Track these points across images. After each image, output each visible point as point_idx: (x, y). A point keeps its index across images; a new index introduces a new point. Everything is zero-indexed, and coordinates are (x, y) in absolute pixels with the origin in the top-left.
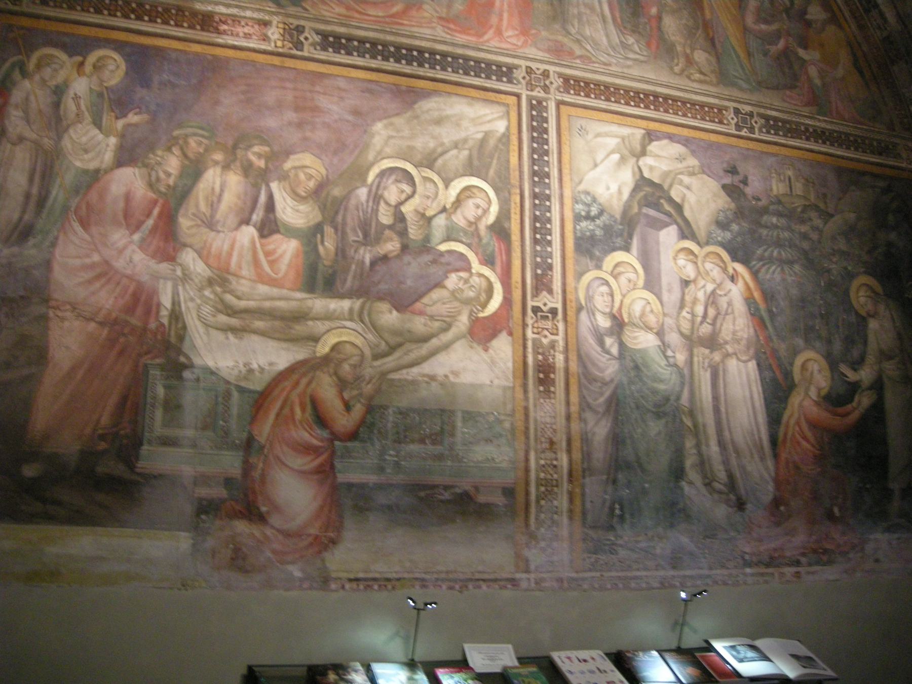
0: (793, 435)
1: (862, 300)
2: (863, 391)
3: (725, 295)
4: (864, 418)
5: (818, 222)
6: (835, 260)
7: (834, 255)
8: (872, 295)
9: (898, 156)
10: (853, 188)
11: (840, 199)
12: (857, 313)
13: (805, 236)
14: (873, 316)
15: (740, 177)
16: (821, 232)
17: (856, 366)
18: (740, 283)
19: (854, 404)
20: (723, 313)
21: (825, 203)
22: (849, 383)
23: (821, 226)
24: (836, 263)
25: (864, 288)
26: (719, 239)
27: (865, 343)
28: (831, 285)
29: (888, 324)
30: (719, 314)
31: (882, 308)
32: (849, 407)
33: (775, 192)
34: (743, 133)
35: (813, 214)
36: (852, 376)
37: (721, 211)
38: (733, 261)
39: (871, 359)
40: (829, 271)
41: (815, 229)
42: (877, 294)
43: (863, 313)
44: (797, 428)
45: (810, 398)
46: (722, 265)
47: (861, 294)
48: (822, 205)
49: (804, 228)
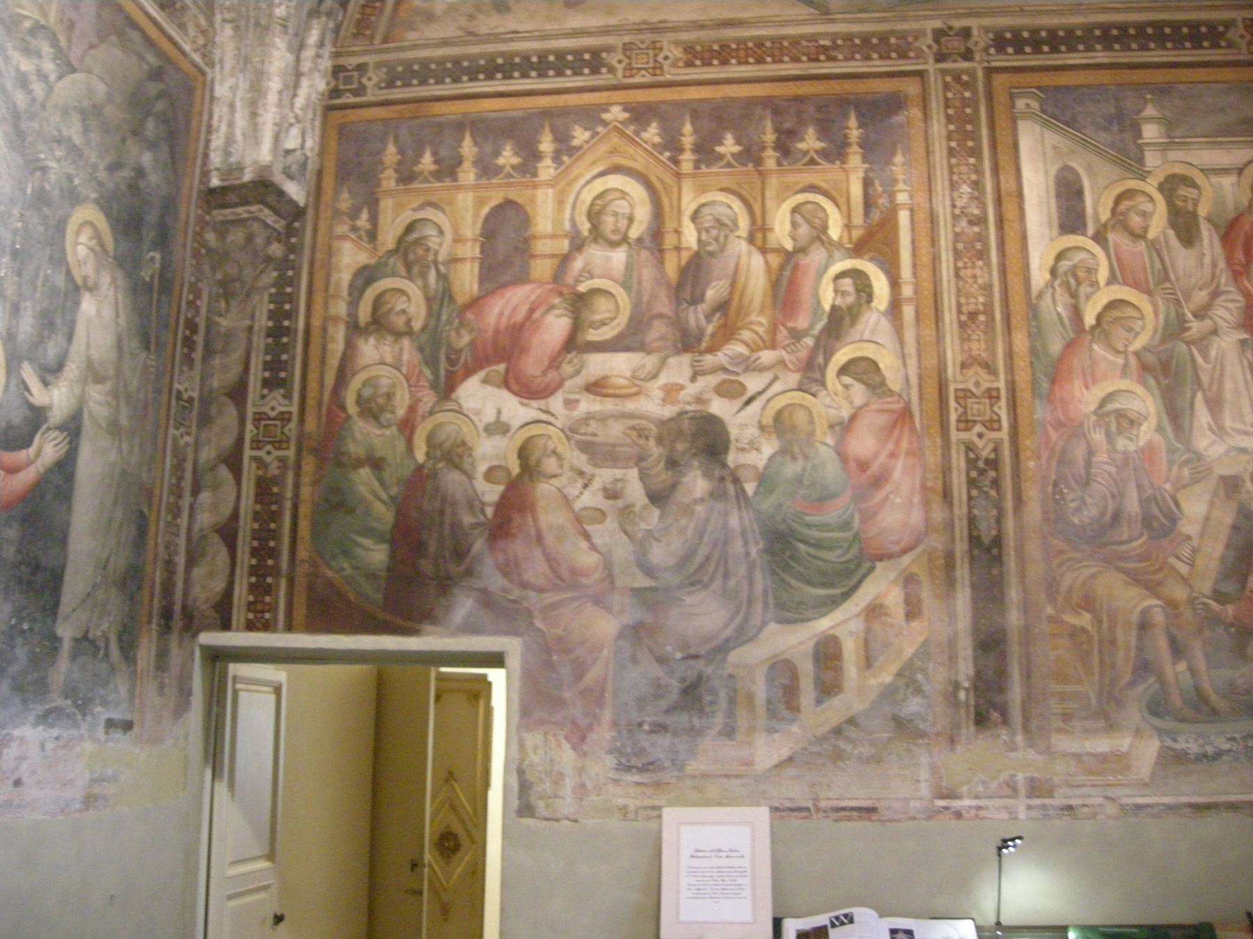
1: (82, 251)
2: (49, 429)
4: (38, 488)
5: (49, 67)
6: (59, 153)
7: (59, 142)
8: (97, 248)
9: (182, 27)
10: (113, 38)
11: (92, 46)
12: (68, 273)
13: (23, 81)
14: (90, 290)
16: (50, 88)
17: (49, 377)
21: (69, 41)
22: (32, 407)
23: (52, 77)
24: (58, 161)
27: (70, 337)
28: (41, 198)
29: (108, 313)
31: (106, 279)
35: (46, 49)
36: (39, 395)
39: (72, 369)
40: (44, 169)
41: (43, 77)
42: (104, 250)
43: (79, 281)
47: (83, 238)
48: (63, 41)
49: (26, 65)
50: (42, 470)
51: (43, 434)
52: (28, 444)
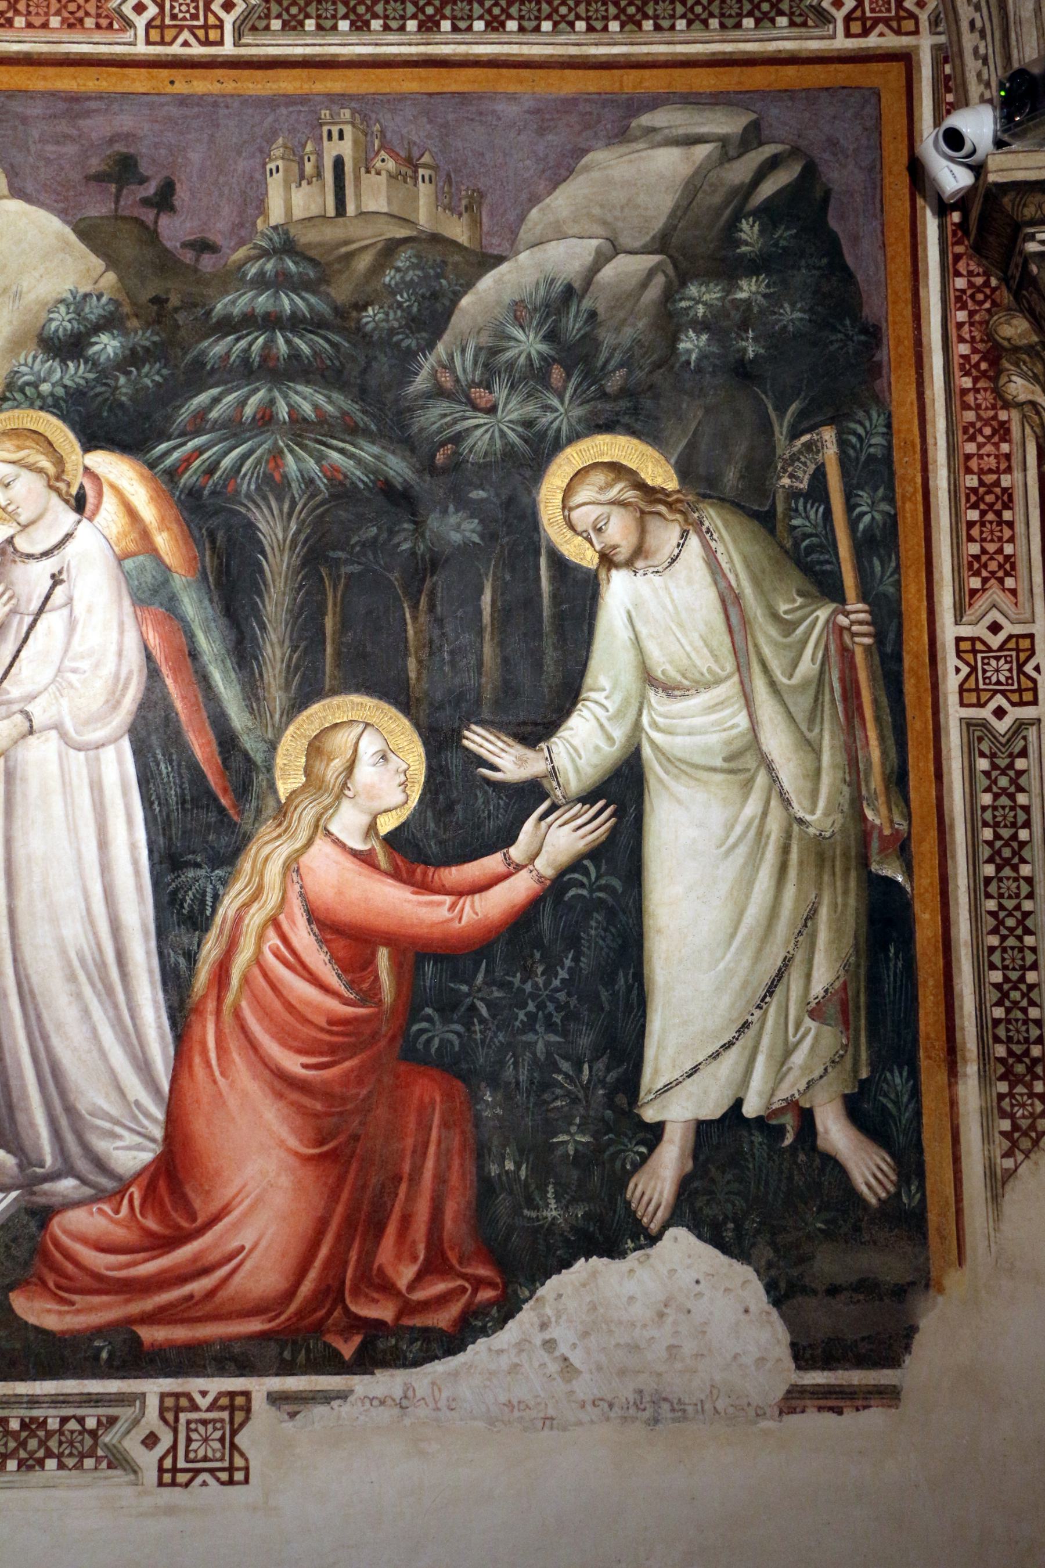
0: (258, 960)
2: (554, 808)
3: (46, 554)
8: (630, 495)
15: (151, 189)
18: (110, 514)
19: (516, 852)
20: (35, 606)
25: (599, 478)
26: (45, 388)
30: (14, 611)
32: (493, 863)
33: (276, 214)
34: (176, 49)
37: (62, 301)
38: (87, 448)
42: (650, 493)
44: (273, 939)
45: (338, 843)
46: (45, 463)
47: (584, 494)
50: (549, 872)
51: (543, 817)
52: (511, 839)
